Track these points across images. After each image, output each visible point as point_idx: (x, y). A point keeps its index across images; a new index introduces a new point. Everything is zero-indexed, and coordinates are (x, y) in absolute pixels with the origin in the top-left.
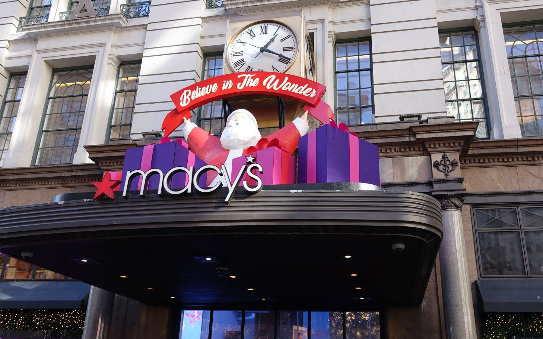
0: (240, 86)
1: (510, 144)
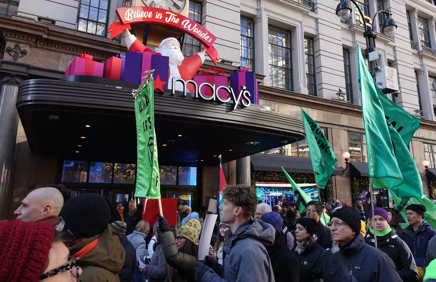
0: (168, 20)
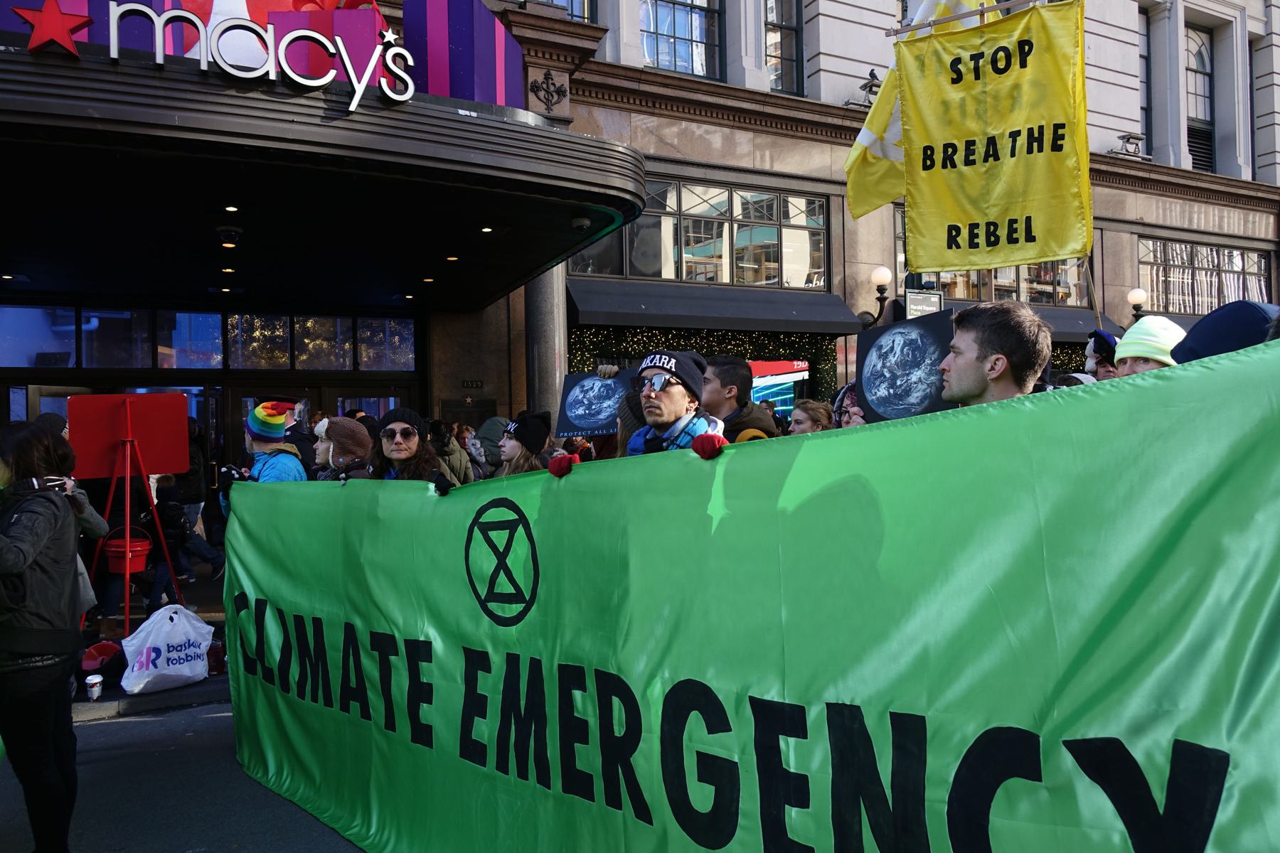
1: (630, 74)
